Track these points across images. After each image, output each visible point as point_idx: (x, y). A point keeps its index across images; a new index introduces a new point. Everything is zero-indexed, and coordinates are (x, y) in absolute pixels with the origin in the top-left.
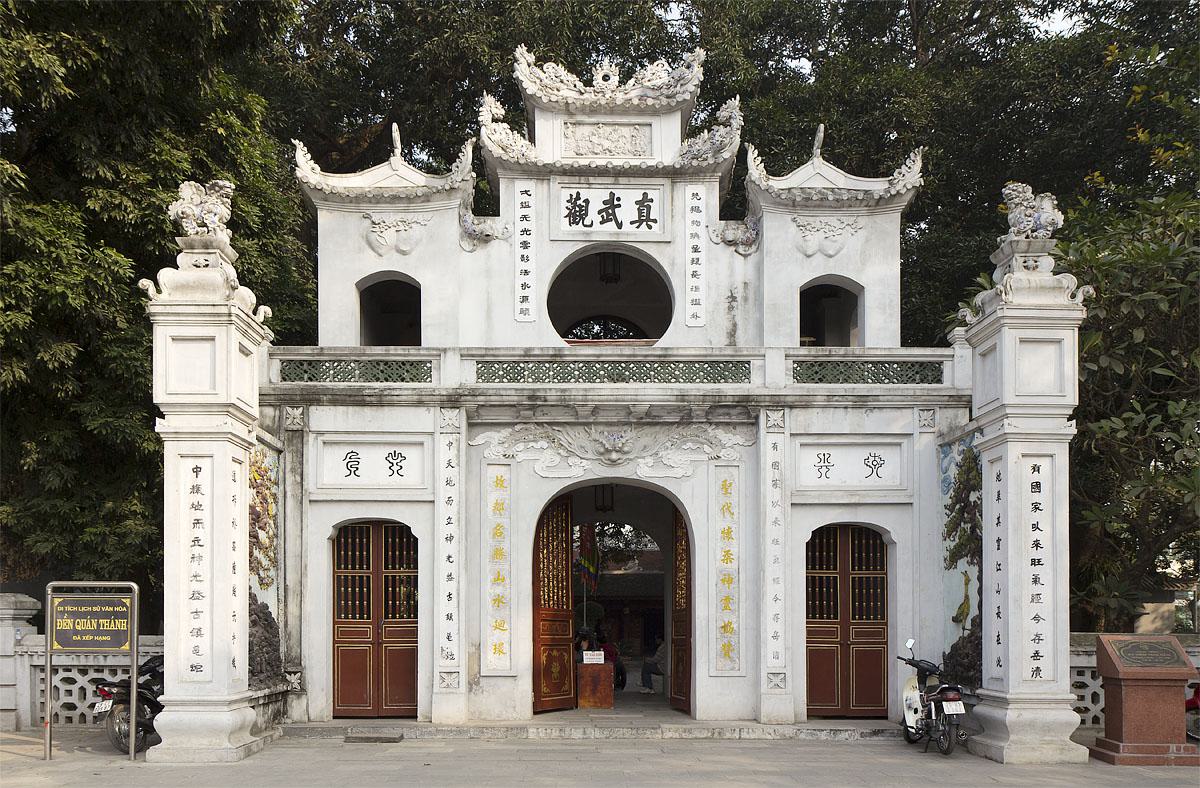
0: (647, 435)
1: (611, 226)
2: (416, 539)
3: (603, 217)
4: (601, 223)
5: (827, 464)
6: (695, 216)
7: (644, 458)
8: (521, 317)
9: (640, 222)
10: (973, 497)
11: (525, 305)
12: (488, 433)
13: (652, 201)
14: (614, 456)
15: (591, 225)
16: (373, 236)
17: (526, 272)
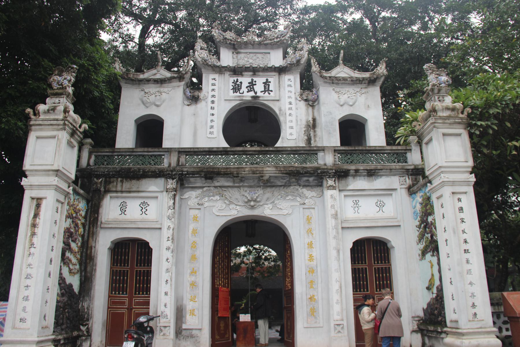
0: (268, 192)
1: (252, 94)
2: (152, 249)
3: (248, 89)
4: (248, 92)
5: (357, 206)
6: (290, 89)
7: (267, 204)
8: (210, 136)
9: (265, 91)
10: (430, 219)
11: (212, 130)
12: (190, 192)
13: (270, 82)
14: (252, 203)
15: (243, 93)
16: (145, 99)
17: (213, 115)
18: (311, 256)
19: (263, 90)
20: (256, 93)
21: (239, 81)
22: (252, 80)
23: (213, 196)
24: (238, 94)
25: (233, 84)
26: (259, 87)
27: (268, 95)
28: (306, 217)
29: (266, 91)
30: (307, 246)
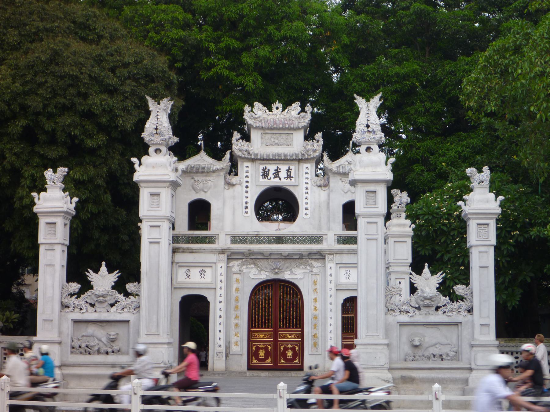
4: (274, 178)
9: (287, 178)
13: (291, 170)
14: (276, 271)
17: (247, 197)
18: (315, 307)
20: (280, 179)
21: (267, 168)
22: (278, 167)
23: (250, 265)
25: (263, 171)
28: (313, 280)
30: (313, 300)
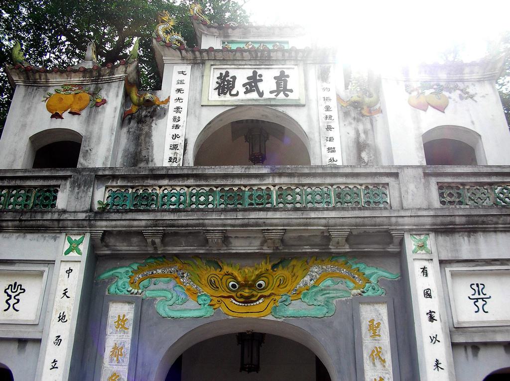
1: (254, 95)
4: (245, 93)
9: (278, 92)
14: (246, 292)
15: (237, 94)
19: (275, 89)
20: (261, 94)
21: (231, 75)
24: (227, 98)
25: (219, 81)
26: (267, 85)
27: (285, 97)
29: (282, 90)
